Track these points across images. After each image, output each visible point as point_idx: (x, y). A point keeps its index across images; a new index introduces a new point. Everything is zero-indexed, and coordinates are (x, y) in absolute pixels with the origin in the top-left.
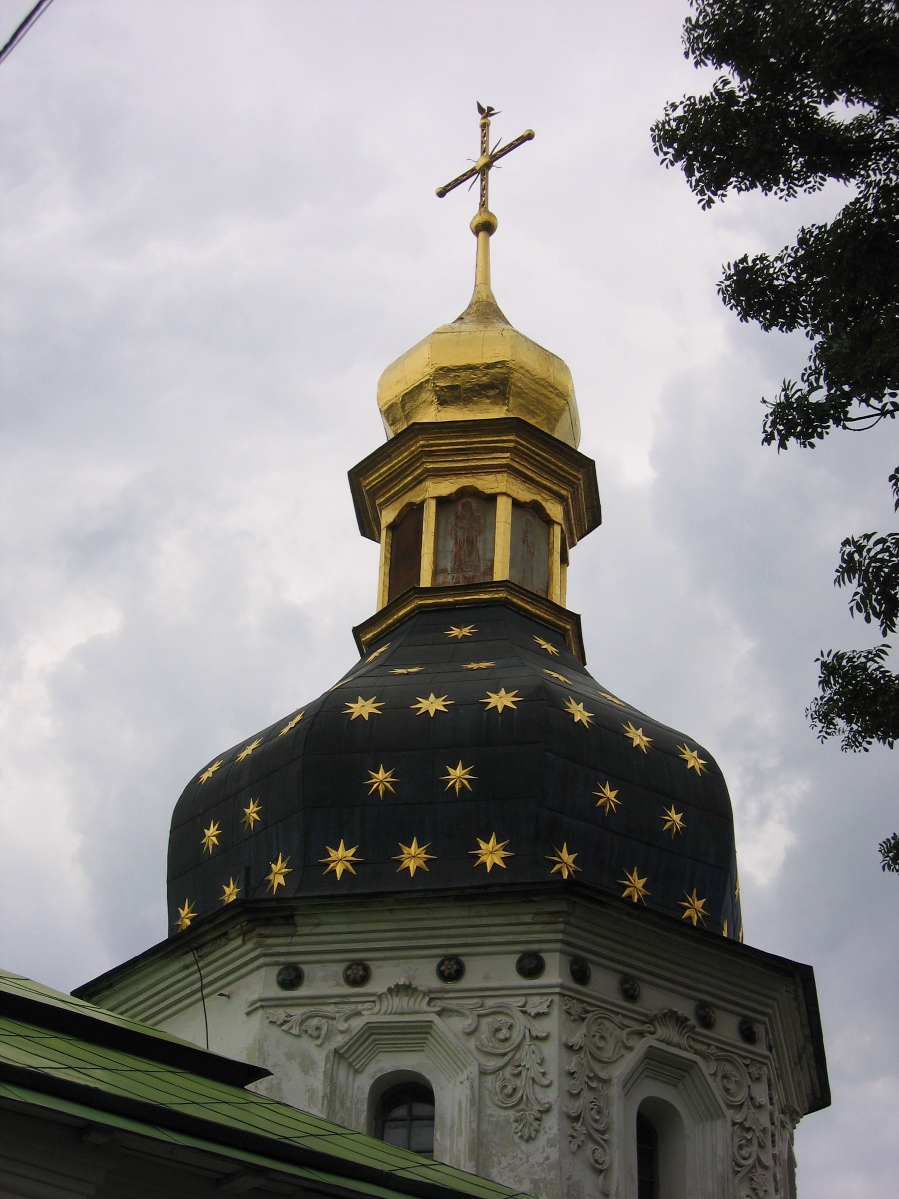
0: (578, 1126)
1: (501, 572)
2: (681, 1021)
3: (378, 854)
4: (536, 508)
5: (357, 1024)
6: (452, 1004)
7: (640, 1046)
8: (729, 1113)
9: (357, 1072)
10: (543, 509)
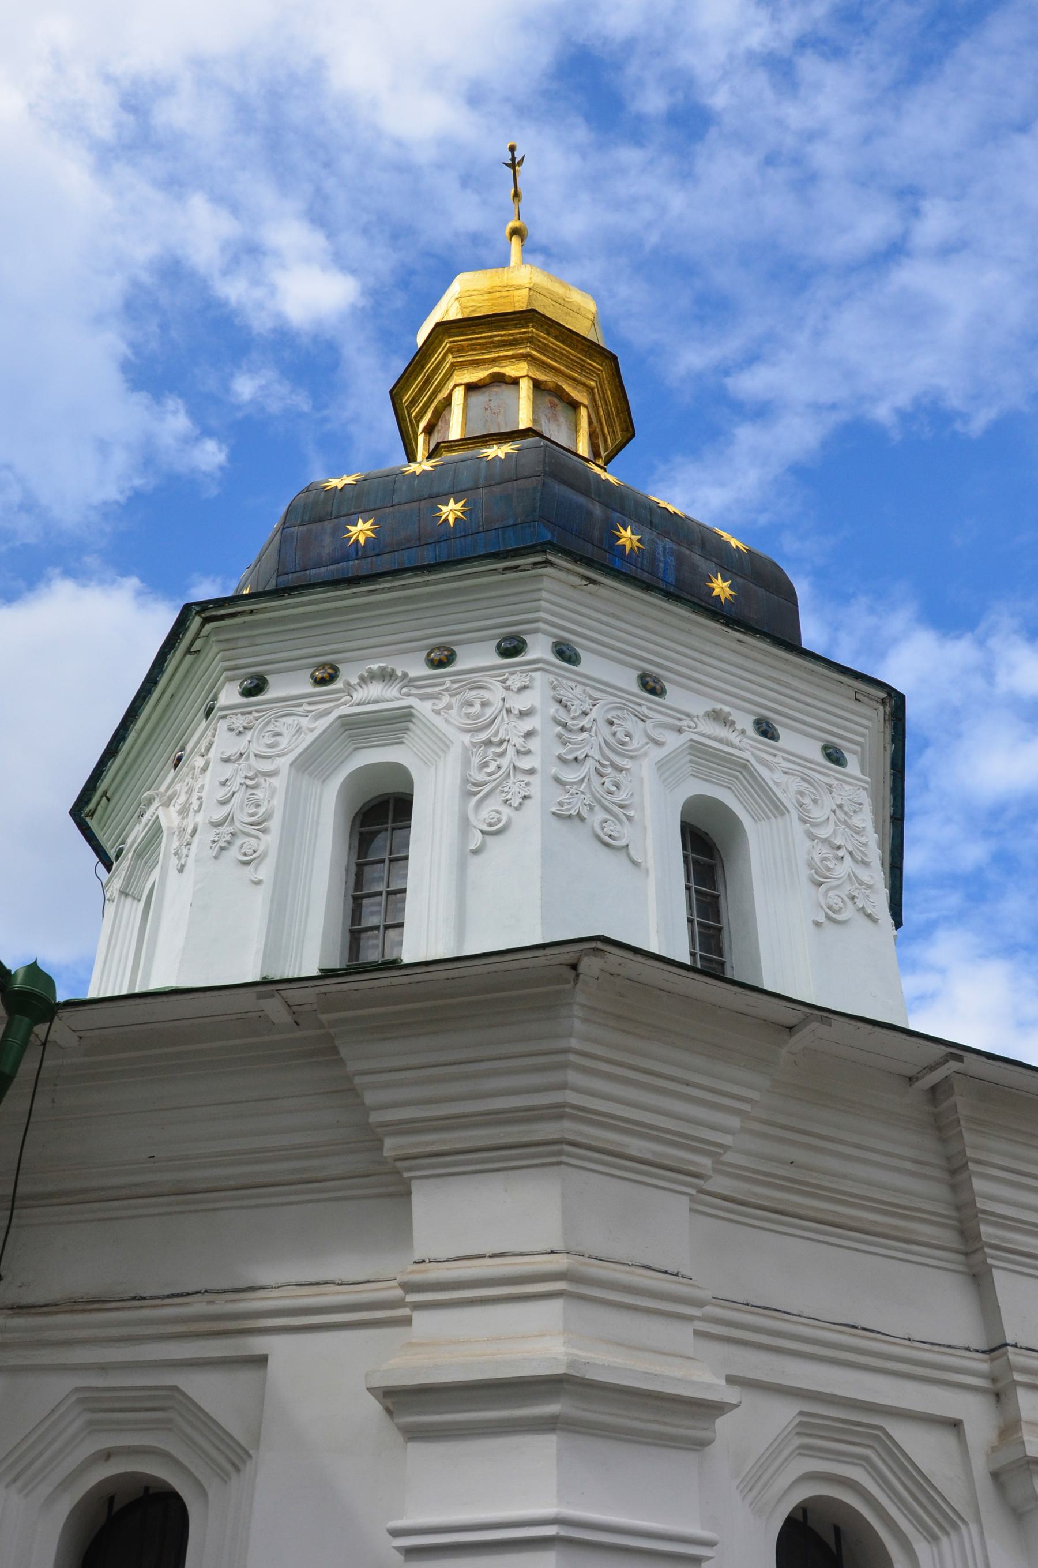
0: (221, 829)
4: (499, 379)
8: (467, 738)
9: (139, 900)
10: (503, 375)
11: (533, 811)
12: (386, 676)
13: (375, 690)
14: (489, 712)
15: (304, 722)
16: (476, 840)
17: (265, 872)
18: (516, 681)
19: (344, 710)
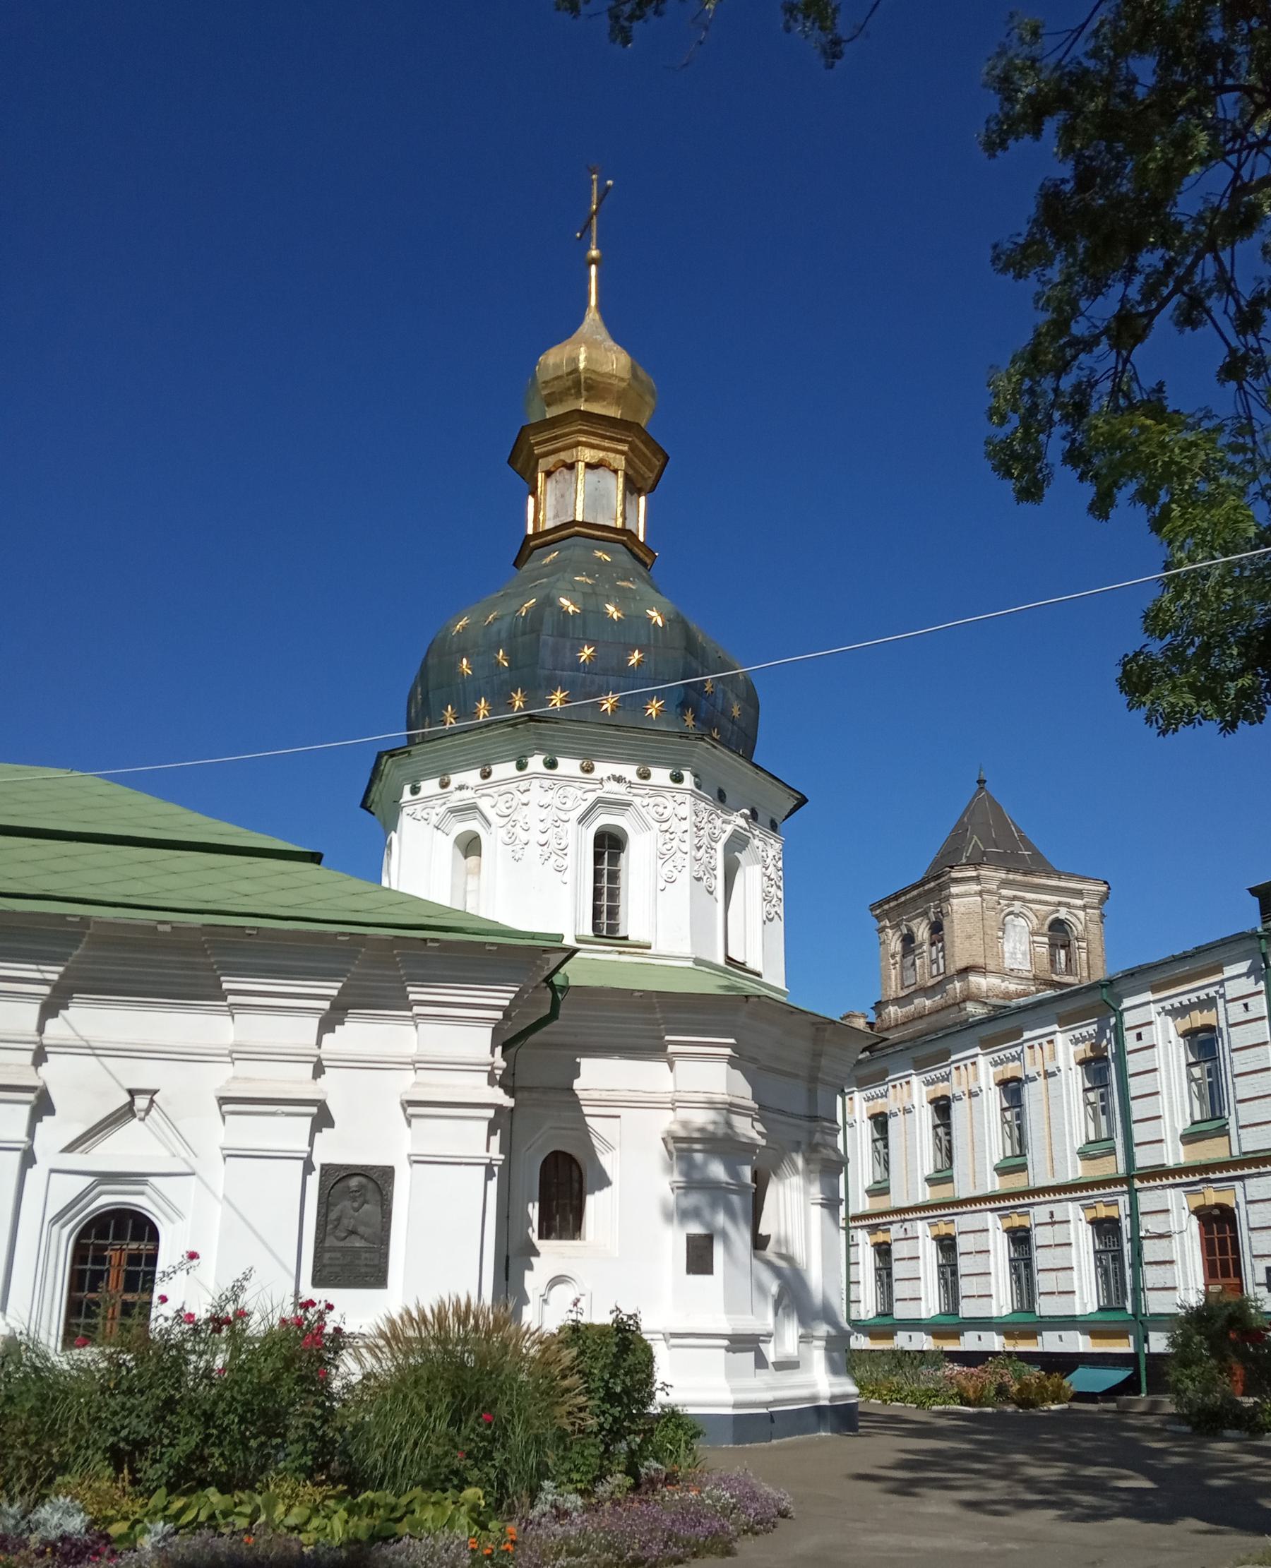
1: (579, 518)
2: (619, 779)
3: (465, 711)
5: (445, 807)
6: (485, 792)
7: (591, 797)
11: (686, 871)
12: (619, 779)
13: (613, 786)
14: (667, 813)
15: (580, 793)
16: (662, 884)
17: (568, 877)
18: (679, 798)
19: (600, 793)
